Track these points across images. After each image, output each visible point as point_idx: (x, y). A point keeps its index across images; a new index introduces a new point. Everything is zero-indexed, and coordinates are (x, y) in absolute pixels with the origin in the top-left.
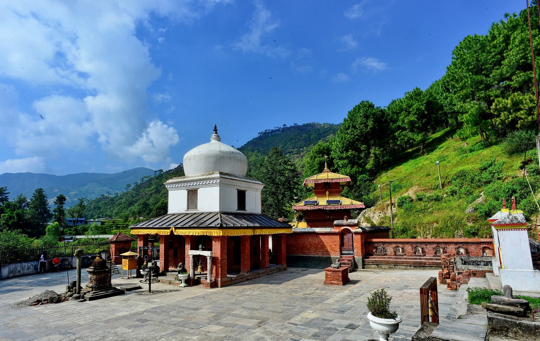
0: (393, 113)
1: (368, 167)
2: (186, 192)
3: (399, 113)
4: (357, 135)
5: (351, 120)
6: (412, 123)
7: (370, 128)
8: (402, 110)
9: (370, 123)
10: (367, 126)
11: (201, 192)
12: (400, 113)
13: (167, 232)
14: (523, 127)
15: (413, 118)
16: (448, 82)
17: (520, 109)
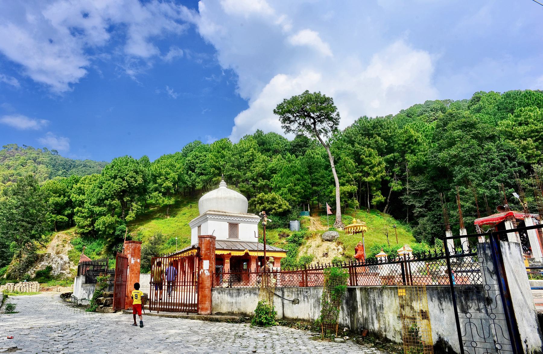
0: (153, 175)
1: (128, 218)
2: (227, 225)
3: (157, 176)
4: (125, 187)
5: (119, 171)
6: (168, 189)
7: (139, 184)
8: (161, 174)
9: (140, 180)
10: (136, 181)
11: (242, 227)
12: (159, 177)
13: (242, 254)
14: (276, 214)
15: (170, 184)
16: (193, 163)
17: (276, 203)
